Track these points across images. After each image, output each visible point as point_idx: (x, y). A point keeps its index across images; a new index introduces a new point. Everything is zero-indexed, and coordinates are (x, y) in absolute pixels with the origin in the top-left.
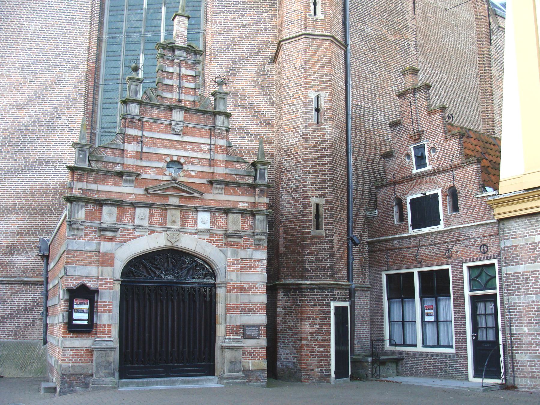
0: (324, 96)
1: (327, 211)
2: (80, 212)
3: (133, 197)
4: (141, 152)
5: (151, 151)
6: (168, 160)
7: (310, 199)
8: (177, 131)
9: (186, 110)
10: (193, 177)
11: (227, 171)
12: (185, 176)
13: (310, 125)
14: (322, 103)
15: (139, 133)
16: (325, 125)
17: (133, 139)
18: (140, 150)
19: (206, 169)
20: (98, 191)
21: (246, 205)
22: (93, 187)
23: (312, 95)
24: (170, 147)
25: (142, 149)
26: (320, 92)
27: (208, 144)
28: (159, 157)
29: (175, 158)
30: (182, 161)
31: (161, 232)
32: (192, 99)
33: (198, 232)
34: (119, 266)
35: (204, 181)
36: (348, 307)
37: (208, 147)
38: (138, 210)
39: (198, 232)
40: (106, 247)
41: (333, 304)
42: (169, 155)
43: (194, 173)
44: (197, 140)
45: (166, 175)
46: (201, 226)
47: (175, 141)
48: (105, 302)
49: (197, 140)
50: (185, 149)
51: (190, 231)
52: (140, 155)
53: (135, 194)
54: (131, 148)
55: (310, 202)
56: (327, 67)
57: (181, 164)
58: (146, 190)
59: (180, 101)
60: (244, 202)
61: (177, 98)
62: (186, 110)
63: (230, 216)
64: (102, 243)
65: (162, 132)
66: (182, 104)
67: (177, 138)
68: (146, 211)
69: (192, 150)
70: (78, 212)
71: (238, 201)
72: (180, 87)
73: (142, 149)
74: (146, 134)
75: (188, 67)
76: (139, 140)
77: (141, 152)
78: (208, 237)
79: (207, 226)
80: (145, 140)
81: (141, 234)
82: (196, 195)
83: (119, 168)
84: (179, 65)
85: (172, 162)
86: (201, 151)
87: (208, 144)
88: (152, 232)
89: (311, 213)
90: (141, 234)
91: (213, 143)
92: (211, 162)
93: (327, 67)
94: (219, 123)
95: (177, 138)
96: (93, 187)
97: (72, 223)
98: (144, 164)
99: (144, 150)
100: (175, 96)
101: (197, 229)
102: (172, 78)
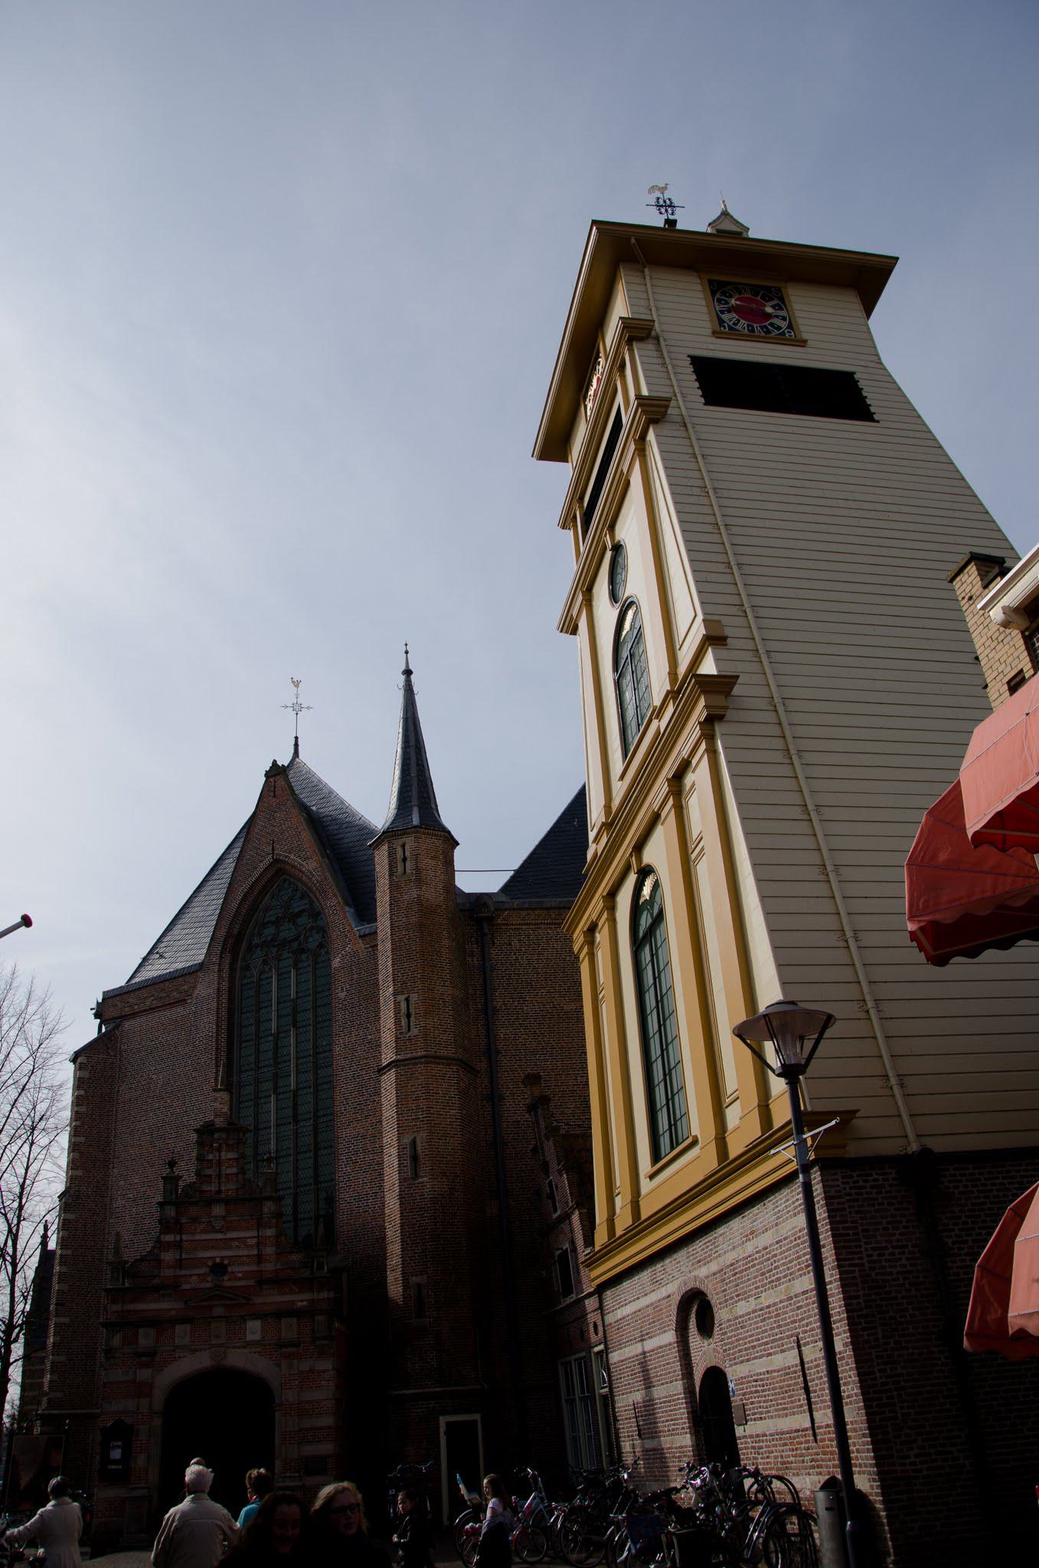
0: (421, 1138)
1: (430, 1291)
2: (115, 1338)
3: (174, 1313)
4: (181, 1260)
5: (192, 1256)
6: (210, 1263)
7: (408, 1279)
8: (218, 1228)
9: (227, 1202)
10: (240, 1279)
11: (279, 1266)
12: (229, 1280)
13: (405, 1180)
14: (419, 1148)
15: (178, 1238)
16: (422, 1177)
17: (168, 1246)
18: (178, 1257)
19: (254, 1268)
20: (136, 1311)
21: (305, 1303)
22: (131, 1307)
23: (407, 1140)
24: (213, 1248)
25: (181, 1255)
26: (416, 1134)
27: (255, 1237)
28: (202, 1262)
29: (218, 1260)
30: (226, 1262)
31: (205, 1350)
32: (235, 1187)
33: (248, 1345)
34: (159, 1397)
35: (251, 1282)
36: (477, 1421)
37: (255, 1240)
38: (179, 1328)
39: (248, 1345)
40: (144, 1374)
41: (443, 1420)
42: (211, 1258)
43: (240, 1275)
44: (242, 1234)
45: (208, 1281)
46: (250, 1337)
47: (216, 1240)
48: (141, 1440)
49: (242, 1234)
50: (231, 1248)
51: (238, 1345)
52: (180, 1264)
53: (175, 1309)
54: (168, 1256)
55: (409, 1283)
56: (423, 1099)
57: (226, 1267)
58: (186, 1303)
59: (219, 1192)
60: (302, 1301)
61: (217, 1189)
62: (227, 1202)
63: (284, 1321)
64: (138, 1371)
65: (204, 1231)
66: (223, 1196)
67: (219, 1236)
68: (188, 1327)
69: (238, 1247)
70: (113, 1338)
71: (293, 1301)
72: (219, 1176)
73: (181, 1255)
74: (185, 1237)
75: (230, 1148)
76: (178, 1246)
77: (181, 1260)
78: (259, 1349)
79: (257, 1337)
80: (185, 1245)
81: (182, 1355)
82: (243, 1301)
83: (156, 1281)
84: (219, 1150)
85: (215, 1264)
86: (247, 1246)
87: (255, 1237)
88: (196, 1351)
89: (411, 1297)
90: (182, 1355)
91: (260, 1234)
92: (260, 1259)
93: (423, 1099)
94: (266, 1210)
95: (219, 1236)
96: (131, 1307)
97: (109, 1352)
98: (183, 1272)
99: (184, 1256)
100: (213, 1188)
101: (245, 1342)
102: (211, 1167)
